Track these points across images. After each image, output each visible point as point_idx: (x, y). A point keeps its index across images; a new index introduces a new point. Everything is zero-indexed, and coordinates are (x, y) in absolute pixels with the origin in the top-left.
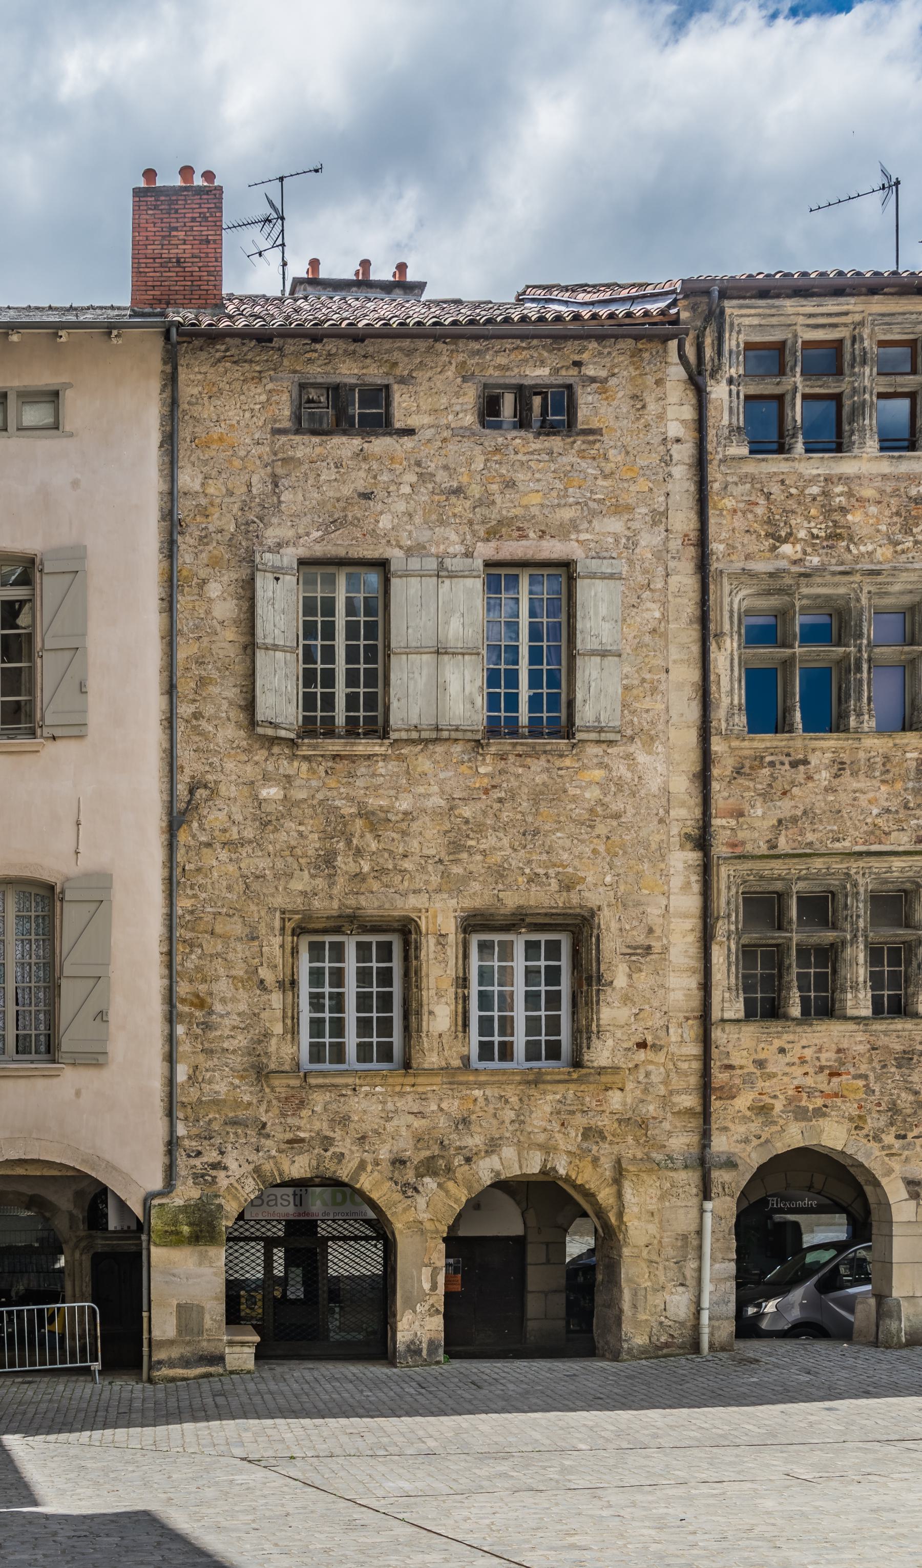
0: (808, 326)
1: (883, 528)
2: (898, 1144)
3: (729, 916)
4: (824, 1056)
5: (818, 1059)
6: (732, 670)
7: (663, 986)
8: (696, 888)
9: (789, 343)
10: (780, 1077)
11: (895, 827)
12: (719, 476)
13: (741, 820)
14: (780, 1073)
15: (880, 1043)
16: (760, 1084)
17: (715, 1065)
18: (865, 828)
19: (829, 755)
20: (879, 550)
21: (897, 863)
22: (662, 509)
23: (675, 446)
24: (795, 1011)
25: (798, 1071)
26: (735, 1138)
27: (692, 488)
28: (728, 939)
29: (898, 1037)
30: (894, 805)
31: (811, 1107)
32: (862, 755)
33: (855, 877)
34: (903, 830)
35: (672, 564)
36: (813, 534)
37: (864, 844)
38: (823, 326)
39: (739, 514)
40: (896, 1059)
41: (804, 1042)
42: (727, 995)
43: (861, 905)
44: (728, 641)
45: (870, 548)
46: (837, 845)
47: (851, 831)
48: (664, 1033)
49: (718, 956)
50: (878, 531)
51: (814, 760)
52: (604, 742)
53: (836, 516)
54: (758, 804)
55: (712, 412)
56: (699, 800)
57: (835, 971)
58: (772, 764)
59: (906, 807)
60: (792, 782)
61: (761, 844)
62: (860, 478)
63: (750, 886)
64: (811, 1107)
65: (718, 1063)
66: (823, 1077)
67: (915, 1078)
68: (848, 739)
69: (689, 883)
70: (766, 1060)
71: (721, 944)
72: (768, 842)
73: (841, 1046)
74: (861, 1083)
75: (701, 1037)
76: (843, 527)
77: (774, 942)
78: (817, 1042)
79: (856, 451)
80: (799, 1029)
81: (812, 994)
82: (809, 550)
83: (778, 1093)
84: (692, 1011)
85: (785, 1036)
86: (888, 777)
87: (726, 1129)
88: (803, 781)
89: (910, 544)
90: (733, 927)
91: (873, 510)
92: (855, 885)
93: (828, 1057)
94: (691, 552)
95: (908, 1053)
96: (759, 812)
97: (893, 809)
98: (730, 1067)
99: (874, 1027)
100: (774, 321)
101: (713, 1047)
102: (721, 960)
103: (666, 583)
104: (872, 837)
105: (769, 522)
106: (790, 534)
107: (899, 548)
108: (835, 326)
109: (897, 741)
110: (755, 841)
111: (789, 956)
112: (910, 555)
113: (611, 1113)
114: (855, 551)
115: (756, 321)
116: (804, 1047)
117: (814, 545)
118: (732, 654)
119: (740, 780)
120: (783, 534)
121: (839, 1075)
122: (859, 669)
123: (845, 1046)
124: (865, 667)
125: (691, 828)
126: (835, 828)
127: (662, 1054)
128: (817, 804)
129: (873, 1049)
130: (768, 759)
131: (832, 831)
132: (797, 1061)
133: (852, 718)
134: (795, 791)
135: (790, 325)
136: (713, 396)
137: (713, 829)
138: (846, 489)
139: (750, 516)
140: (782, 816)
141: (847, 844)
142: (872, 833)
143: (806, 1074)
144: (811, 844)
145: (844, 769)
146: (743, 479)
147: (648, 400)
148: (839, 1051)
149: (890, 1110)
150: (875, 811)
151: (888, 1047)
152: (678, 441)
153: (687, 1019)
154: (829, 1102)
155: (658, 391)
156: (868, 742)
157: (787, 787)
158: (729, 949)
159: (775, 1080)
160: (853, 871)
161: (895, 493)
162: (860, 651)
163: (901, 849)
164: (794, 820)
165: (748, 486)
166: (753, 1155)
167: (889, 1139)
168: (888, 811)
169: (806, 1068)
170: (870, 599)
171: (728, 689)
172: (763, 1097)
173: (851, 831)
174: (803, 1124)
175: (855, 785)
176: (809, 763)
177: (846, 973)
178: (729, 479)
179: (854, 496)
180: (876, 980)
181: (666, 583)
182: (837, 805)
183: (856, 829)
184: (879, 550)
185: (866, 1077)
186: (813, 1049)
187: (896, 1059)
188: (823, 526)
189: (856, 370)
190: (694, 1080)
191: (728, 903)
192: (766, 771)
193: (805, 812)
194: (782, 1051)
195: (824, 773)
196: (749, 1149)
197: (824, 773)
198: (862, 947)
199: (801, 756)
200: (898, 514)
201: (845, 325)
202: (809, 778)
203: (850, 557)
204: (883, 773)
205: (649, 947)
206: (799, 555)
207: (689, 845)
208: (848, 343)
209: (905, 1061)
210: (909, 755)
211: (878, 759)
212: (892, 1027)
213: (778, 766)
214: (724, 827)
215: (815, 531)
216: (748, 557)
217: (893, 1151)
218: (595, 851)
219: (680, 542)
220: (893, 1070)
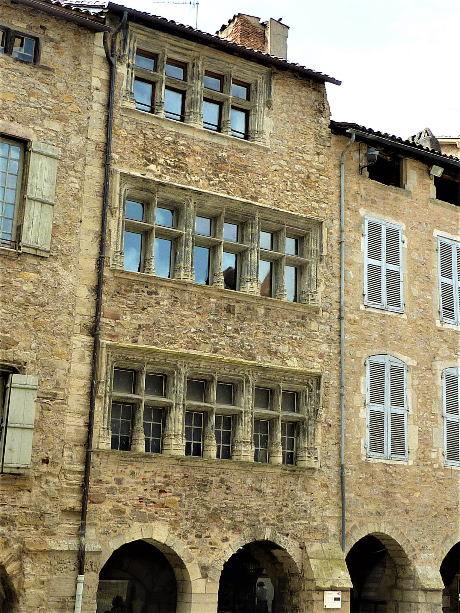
0: (171, 50)
1: (204, 169)
3: (107, 381)
4: (158, 479)
7: (62, 422)
9: (160, 56)
14: (131, 488)
17: (92, 480)
24: (141, 448)
28: (105, 396)
36: (167, 163)
38: (179, 53)
41: (146, 469)
42: (102, 432)
43: (182, 386)
45: (197, 178)
48: (60, 456)
49: (98, 407)
50: (201, 170)
52: (38, 256)
56: (94, 305)
57: (164, 425)
63: (120, 364)
65: (93, 479)
66: (155, 493)
70: (123, 479)
71: (100, 398)
73: (167, 474)
75: (83, 460)
76: (183, 163)
77: (131, 401)
78: (153, 469)
81: (151, 438)
82: (165, 171)
85: (135, 464)
86: (200, 311)
88: (154, 305)
90: (108, 389)
92: (180, 373)
93: (159, 480)
98: (100, 481)
101: (91, 467)
107: (211, 182)
108: (185, 55)
110: (124, 335)
111: (139, 411)
113: (21, 507)
114: (189, 179)
116: (146, 472)
124: (191, 244)
127: (58, 468)
132: (140, 480)
133: (182, 272)
134: (149, 309)
135: (162, 46)
138: (186, 143)
145: (177, 301)
157: (145, 306)
164: (148, 327)
170: (195, 207)
176: (158, 294)
177: (170, 425)
180: (188, 433)
186: (151, 474)
188: (173, 160)
189: (194, 81)
191: (107, 373)
193: (154, 324)
194: (133, 473)
195: (165, 303)
198: (181, 411)
201: (190, 56)
202: (158, 303)
205: (56, 394)
206: (159, 173)
208: (190, 66)
212: (197, 464)
215: (169, 162)
218: (26, 326)
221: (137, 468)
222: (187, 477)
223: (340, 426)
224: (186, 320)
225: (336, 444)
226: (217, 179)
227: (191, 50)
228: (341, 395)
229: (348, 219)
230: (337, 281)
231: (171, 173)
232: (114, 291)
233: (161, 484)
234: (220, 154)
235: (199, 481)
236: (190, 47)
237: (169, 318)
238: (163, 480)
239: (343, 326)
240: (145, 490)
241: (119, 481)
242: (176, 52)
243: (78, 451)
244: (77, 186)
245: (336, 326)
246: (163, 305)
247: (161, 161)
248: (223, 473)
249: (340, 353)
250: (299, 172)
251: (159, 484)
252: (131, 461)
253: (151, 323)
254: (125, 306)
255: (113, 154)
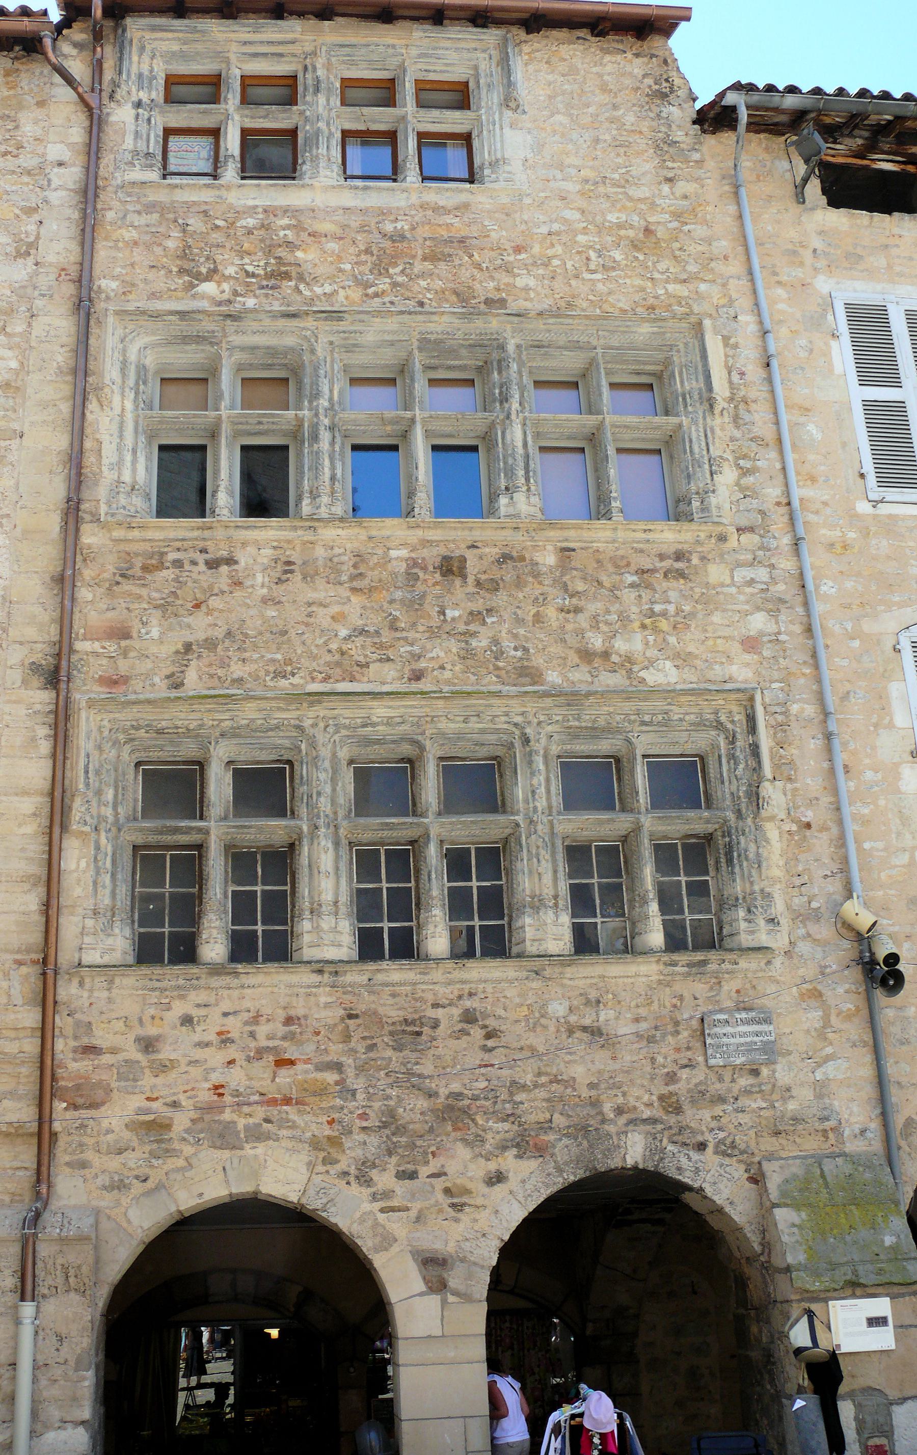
1: (348, 267)
2: (401, 1188)
4: (262, 1030)
5: (252, 1035)
6: (121, 437)
8: (45, 747)
10: (183, 1068)
11: (375, 656)
12: (116, 204)
13: (124, 643)
14: (184, 1061)
15: (361, 1008)
16: (148, 1081)
18: (328, 658)
19: (267, 552)
20: (342, 293)
21: (380, 710)
22: (32, 239)
23: (56, 170)
25: (216, 1057)
26: (99, 1181)
27: (76, 215)
29: (394, 995)
30: (374, 621)
31: (241, 1123)
32: (320, 552)
33: (312, 731)
34: (389, 660)
35: (39, 303)
36: (246, 271)
37: (325, 680)
39: (142, 247)
40: (391, 1034)
41: (226, 1006)
42: (90, 923)
44: (117, 399)
45: (328, 289)
46: (283, 683)
47: (305, 662)
50: (341, 270)
51: (243, 559)
53: (281, 252)
54: (154, 622)
55: (110, 136)
58: (178, 564)
59: (393, 627)
60: (211, 587)
61: (157, 680)
62: (313, 211)
64: (241, 1123)
66: (262, 1072)
67: (427, 1067)
68: (295, 528)
69: (33, 739)
70: (158, 1038)
72: (168, 677)
73: (292, 1013)
74: (331, 1077)
78: (247, 1004)
79: (307, 181)
80: (216, 982)
83: (182, 1098)
84: (28, 951)
87: (84, 1165)
88: (226, 588)
89: (387, 287)
91: (332, 246)
92: (313, 745)
94: (69, 289)
95: (413, 1023)
96: (155, 633)
97: (372, 629)
99: (349, 978)
100: (199, 47)
102: (83, 864)
103: (30, 325)
104: (338, 671)
105: (184, 256)
106: (215, 271)
107: (371, 291)
109: (374, 533)
112: (387, 299)
114: (307, 293)
115: (175, 47)
116: (226, 1014)
117: (248, 284)
118: (122, 416)
119: (127, 586)
120: (204, 270)
121: (292, 1063)
122: (315, 437)
123: (300, 1012)
125: (41, 654)
126: (279, 656)
128: (249, 622)
129: (351, 1017)
130: (172, 556)
131: (273, 661)
133: (306, 502)
134: (214, 602)
136: (112, 119)
137: (74, 658)
138: (293, 222)
139: (158, 250)
140: (190, 639)
141: (296, 680)
142: (338, 664)
143: (231, 1062)
144: (239, 681)
145: (292, 572)
146: (150, 208)
147: (23, 121)
148: (289, 1021)
149: (385, 1125)
150: (343, 633)
151: (375, 1013)
152: (60, 164)
153: (20, 963)
154: (274, 1112)
155: (39, 113)
156: (329, 533)
158: (98, 848)
159: (173, 1074)
160: (307, 723)
161: (363, 228)
162: (317, 415)
163: (386, 688)
164: (210, 644)
165: (156, 216)
166: (133, 1214)
167: (384, 1179)
168: (362, 632)
169: (232, 1052)
171: (114, 459)
172: (154, 1105)
173: (305, 662)
174: (226, 1154)
175: (311, 595)
176: (236, 562)
178: (130, 207)
179: (305, 230)
181: (30, 325)
182: (281, 623)
183: (314, 658)
184: (342, 293)
185: (338, 1067)
186: (246, 1016)
187: (391, 1034)
190: (28, 1073)
192: (169, 574)
193: (229, 634)
194: (187, 1020)
195: (259, 578)
196: (125, 1201)
197: (259, 578)
199: (224, 553)
200: (368, 251)
203: (299, 298)
204: (353, 578)
206: (225, 296)
207: (36, 681)
209: (408, 1038)
210: (393, 553)
211: (345, 558)
213: (187, 567)
214: (96, 654)
215: (250, 269)
216: (153, 296)
217: (395, 1203)
219: (53, 277)
220: (389, 1053)
221: (198, 1006)
222: (356, 1016)
223: (840, 822)
224: (321, 611)
225: (833, 874)
226: (388, 280)
227: (293, 42)
228: (829, 737)
229: (781, 306)
230: (773, 455)
231: (258, 292)
232: (114, 574)
233: (276, 1043)
234: (389, 227)
235: (394, 1024)
236: (290, 36)
237: (274, 614)
238: (281, 1030)
239: (808, 560)
240: (230, 1063)
241: (148, 1045)
242: (256, 55)
243: (26, 977)
244: (14, 364)
245: (786, 564)
246: (252, 586)
247: (231, 271)
248: (471, 994)
249: (809, 630)
250: (620, 226)
251: (271, 1044)
252: (179, 987)
253: (219, 633)
254: (146, 606)
255: (103, 283)
